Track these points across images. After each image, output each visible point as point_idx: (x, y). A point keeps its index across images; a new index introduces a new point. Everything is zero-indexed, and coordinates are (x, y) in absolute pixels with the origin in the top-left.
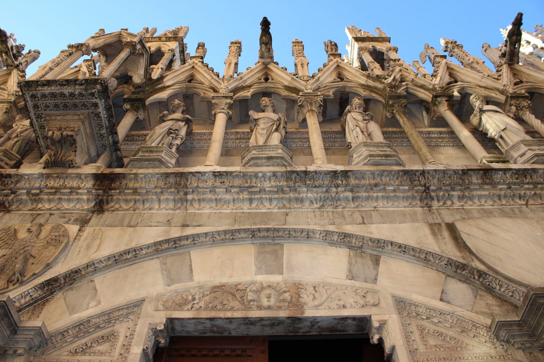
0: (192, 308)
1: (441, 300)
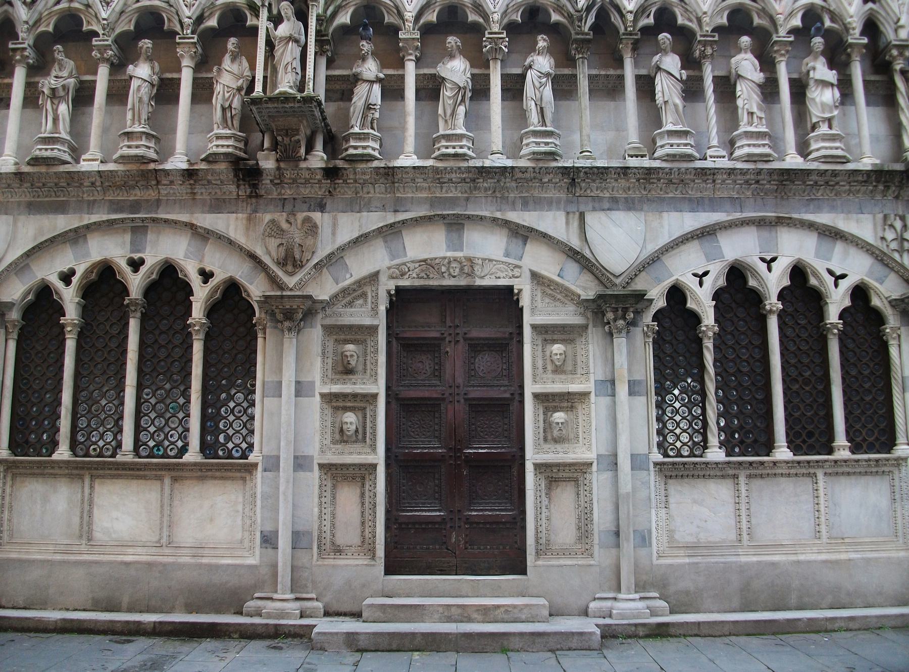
1: (559, 275)
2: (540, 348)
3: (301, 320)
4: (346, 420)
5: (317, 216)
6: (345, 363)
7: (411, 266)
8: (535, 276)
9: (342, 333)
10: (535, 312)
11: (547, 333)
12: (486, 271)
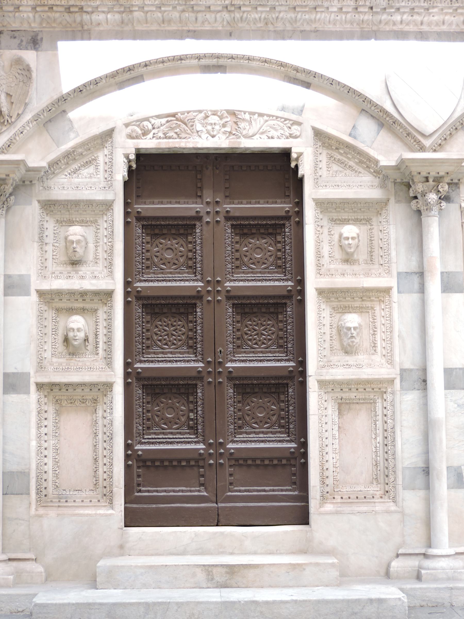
0: (153, 137)
1: (350, 135)
2: (326, 231)
3: (11, 195)
4: (72, 325)
5: (29, 56)
6: (71, 250)
7: (157, 122)
8: (318, 134)
9: (63, 211)
10: (320, 182)
11: (337, 210)
12: (255, 128)
